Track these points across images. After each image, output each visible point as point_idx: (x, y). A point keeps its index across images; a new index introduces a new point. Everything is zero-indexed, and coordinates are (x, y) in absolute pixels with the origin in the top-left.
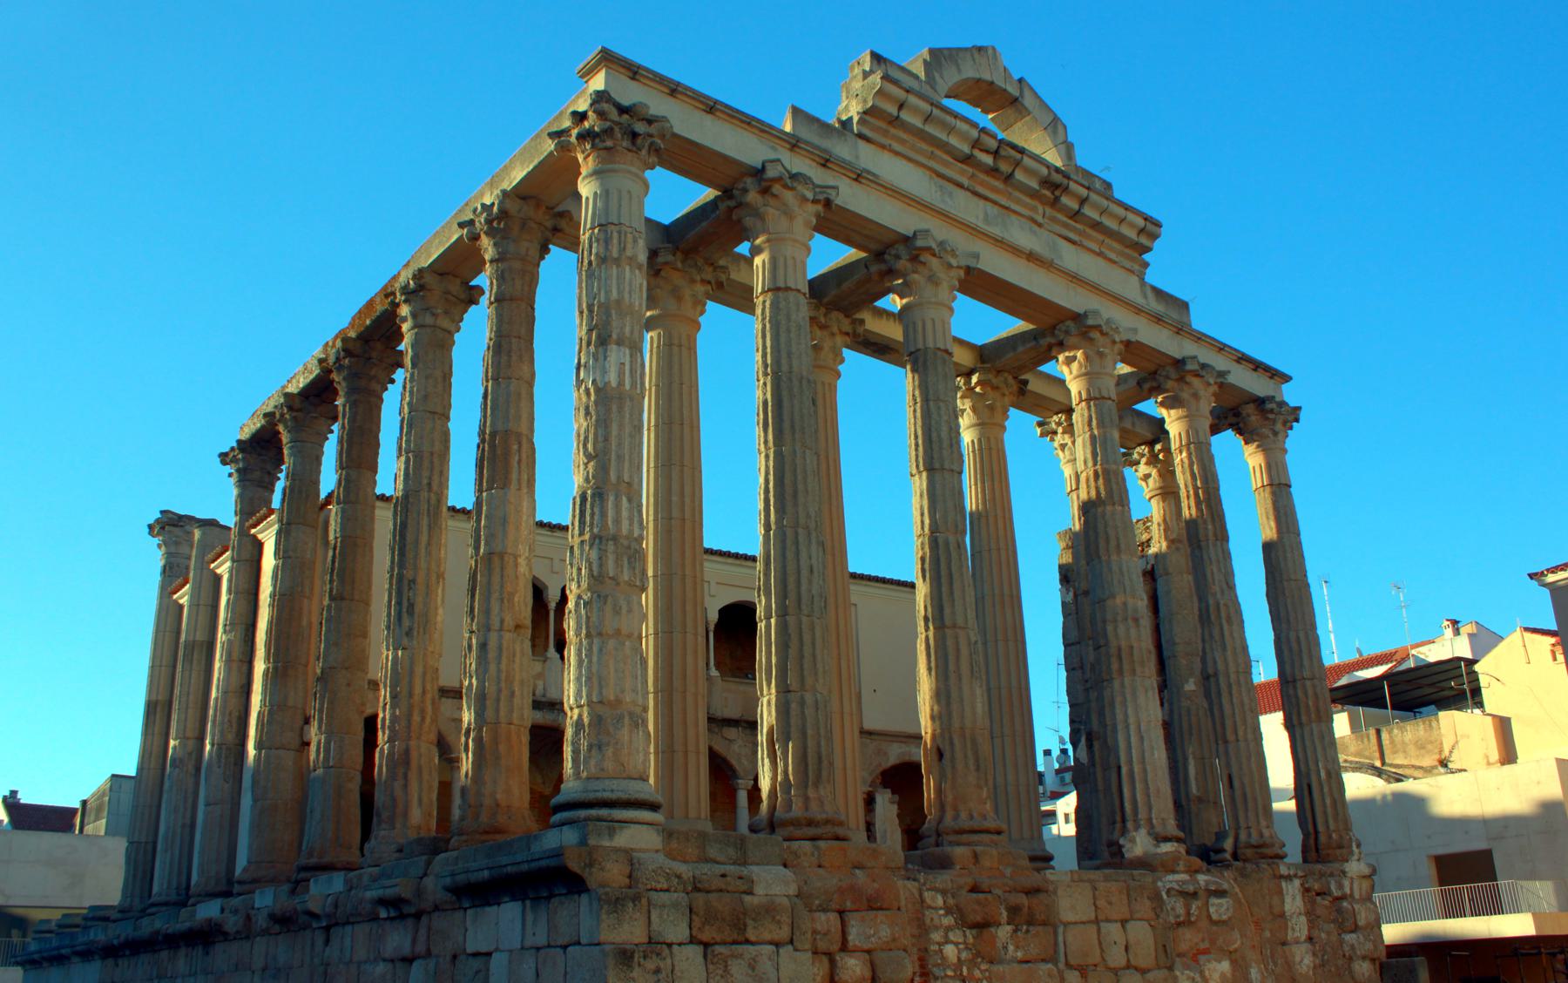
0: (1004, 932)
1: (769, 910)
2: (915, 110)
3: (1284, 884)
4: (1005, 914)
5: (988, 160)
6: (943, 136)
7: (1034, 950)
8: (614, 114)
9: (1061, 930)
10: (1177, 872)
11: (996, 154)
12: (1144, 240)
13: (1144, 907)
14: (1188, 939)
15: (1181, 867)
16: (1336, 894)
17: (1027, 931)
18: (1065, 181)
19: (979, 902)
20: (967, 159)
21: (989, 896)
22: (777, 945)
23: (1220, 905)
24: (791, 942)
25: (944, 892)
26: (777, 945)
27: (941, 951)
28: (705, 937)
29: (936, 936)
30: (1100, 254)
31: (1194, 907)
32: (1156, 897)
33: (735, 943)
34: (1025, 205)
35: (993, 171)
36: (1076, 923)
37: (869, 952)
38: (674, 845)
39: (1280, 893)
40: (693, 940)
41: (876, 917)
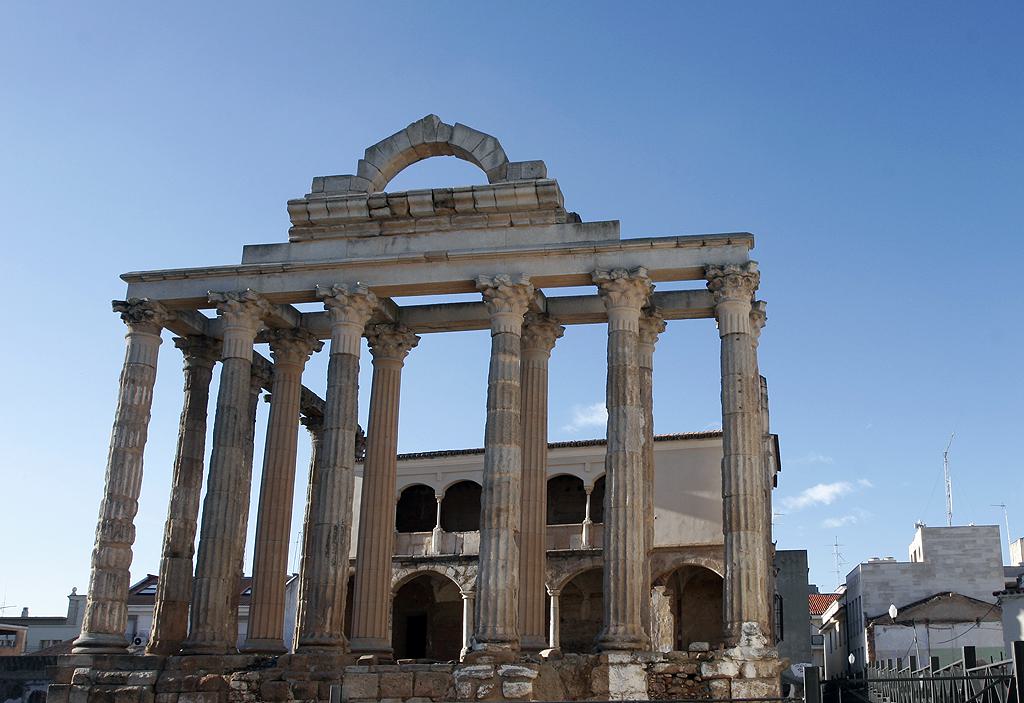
2: (318, 211)
3: (612, 671)
4: (291, 694)
5: (386, 212)
6: (345, 215)
8: (123, 308)
10: (481, 664)
11: (388, 205)
12: (544, 200)
15: (485, 659)
18: (450, 195)
19: (274, 686)
20: (371, 218)
21: (282, 683)
25: (248, 681)
30: (512, 225)
35: (395, 216)
38: (99, 663)
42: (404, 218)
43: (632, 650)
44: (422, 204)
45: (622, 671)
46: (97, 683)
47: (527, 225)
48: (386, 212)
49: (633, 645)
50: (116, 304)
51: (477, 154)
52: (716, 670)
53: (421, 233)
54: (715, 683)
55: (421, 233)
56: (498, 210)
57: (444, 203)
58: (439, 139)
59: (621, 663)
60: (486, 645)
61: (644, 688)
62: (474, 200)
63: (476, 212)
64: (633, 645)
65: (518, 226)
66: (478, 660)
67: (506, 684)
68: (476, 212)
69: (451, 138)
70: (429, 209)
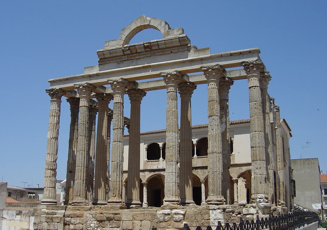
0: (107, 222)
1: (57, 217)
4: (105, 219)
5: (129, 52)
7: (114, 226)
9: (122, 221)
13: (150, 217)
14: (164, 224)
15: (168, 207)
16: (244, 213)
17: (113, 222)
22: (58, 223)
23: (177, 217)
24: (60, 222)
26: (58, 223)
27: (90, 225)
28: (47, 222)
29: (88, 222)
30: (172, 52)
31: (166, 218)
32: (155, 215)
33: (51, 222)
34: (144, 55)
36: (127, 220)
37: (75, 224)
38: (48, 208)
39: (208, 214)
40: (46, 222)
41: (77, 219)
42: (135, 53)
43: (218, 204)
44: (141, 48)
45: (214, 212)
46: (48, 214)
47: (177, 52)
48: (129, 52)
49: (218, 203)
50: (46, 90)
51: (159, 28)
52: (248, 212)
53: (141, 58)
54: (248, 216)
55: (141, 58)
56: (167, 48)
57: (148, 47)
58: (146, 24)
59: (214, 209)
60: (168, 202)
61: (223, 218)
62: (158, 45)
63: (160, 49)
64: (218, 203)
65: (174, 53)
66: (165, 208)
67: (174, 216)
68: (160, 49)
69: (150, 23)
70: (143, 50)
